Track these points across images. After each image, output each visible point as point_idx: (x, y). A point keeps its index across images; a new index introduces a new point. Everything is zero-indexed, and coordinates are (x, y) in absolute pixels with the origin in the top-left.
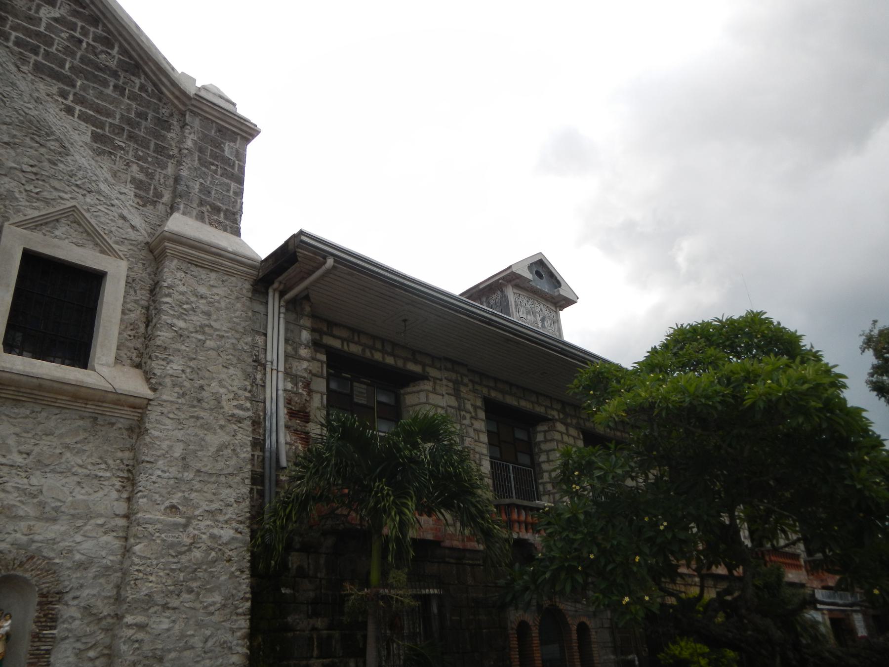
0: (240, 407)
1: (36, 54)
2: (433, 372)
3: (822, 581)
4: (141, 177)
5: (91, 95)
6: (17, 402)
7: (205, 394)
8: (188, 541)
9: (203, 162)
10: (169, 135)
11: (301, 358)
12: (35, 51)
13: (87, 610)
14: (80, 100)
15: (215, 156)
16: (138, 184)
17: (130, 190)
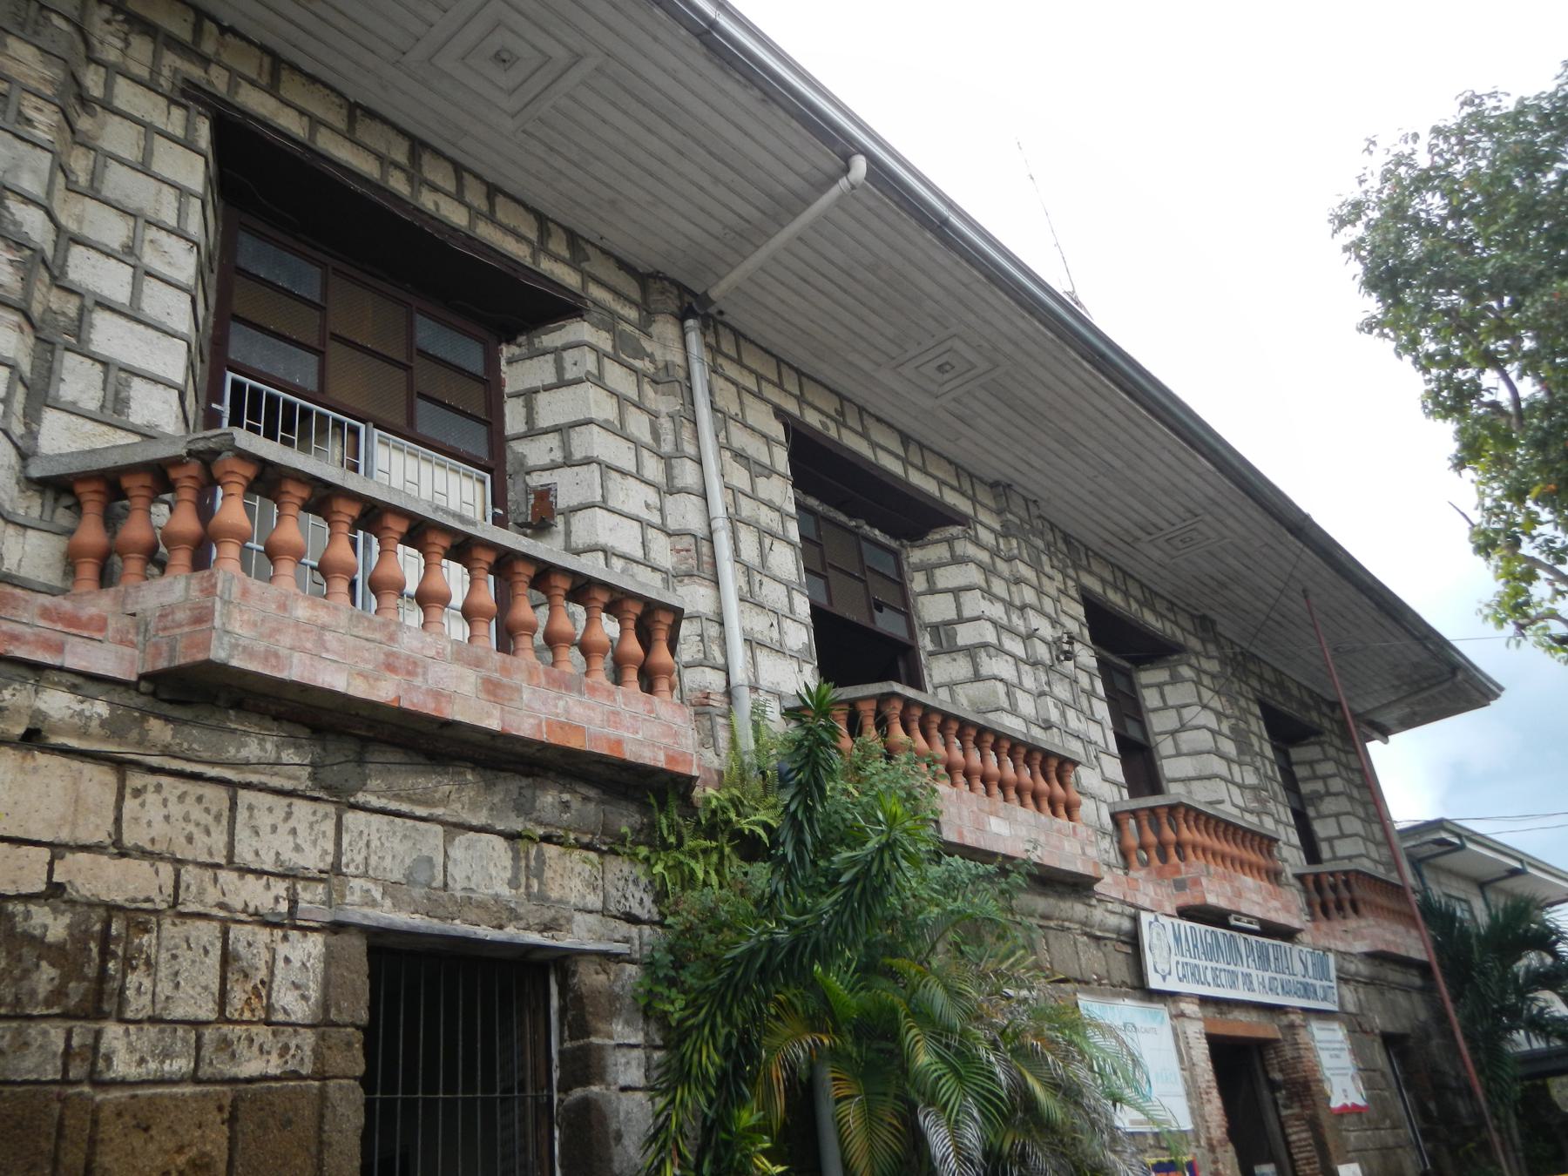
3: (1180, 886)
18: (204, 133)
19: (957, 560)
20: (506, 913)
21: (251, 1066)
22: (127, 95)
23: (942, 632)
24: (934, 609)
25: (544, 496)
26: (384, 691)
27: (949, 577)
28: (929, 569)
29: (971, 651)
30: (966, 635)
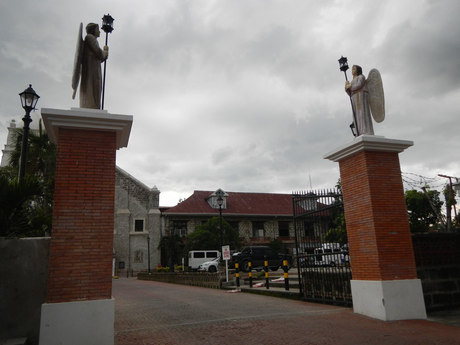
0: (159, 233)
1: (133, 194)
2: (191, 219)
4: (146, 205)
5: (139, 197)
6: (137, 236)
7: (155, 232)
8: (154, 248)
9: (153, 200)
10: (149, 198)
11: (167, 224)
12: (133, 194)
13: (145, 254)
14: (138, 198)
15: (155, 199)
16: (146, 206)
17: (145, 208)
19: (291, 224)
22: (250, 223)
23: (290, 228)
24: (290, 227)
25: (265, 230)
26: (259, 243)
27: (291, 225)
28: (290, 224)
29: (292, 230)
30: (291, 229)
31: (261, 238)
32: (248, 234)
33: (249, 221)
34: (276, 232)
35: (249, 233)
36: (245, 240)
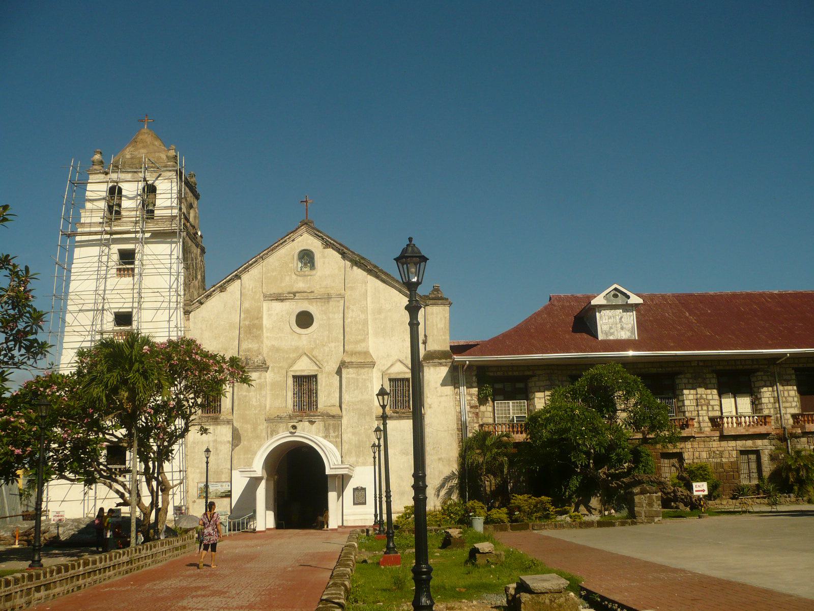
18: (715, 375)
20: (751, 447)
21: (732, 460)
22: (708, 376)
31: (743, 418)
32: (705, 408)
33: (705, 371)
34: (790, 399)
35: (708, 405)
36: (696, 425)
